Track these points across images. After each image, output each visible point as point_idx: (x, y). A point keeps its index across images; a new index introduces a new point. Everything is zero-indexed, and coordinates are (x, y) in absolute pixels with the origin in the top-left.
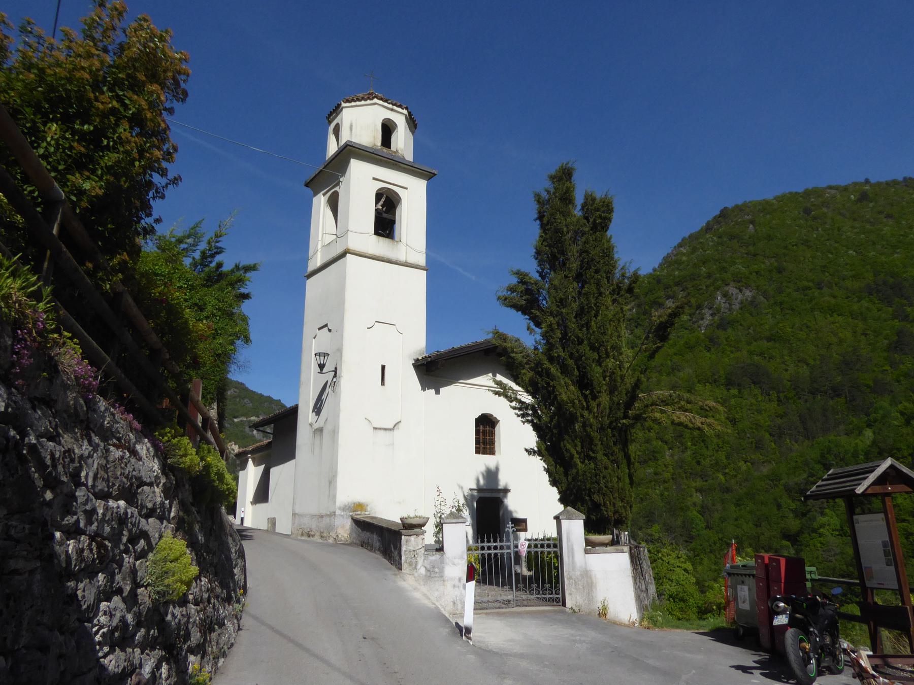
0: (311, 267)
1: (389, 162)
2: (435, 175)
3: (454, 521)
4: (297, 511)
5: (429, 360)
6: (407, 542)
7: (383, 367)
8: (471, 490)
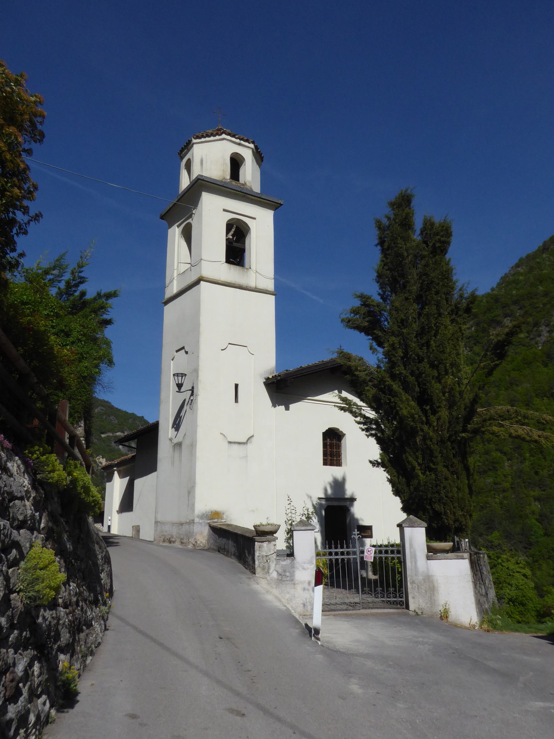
0: (168, 295)
1: (238, 194)
2: (281, 205)
3: (303, 528)
4: (159, 519)
5: (279, 378)
6: (260, 548)
7: (237, 386)
8: (319, 499)
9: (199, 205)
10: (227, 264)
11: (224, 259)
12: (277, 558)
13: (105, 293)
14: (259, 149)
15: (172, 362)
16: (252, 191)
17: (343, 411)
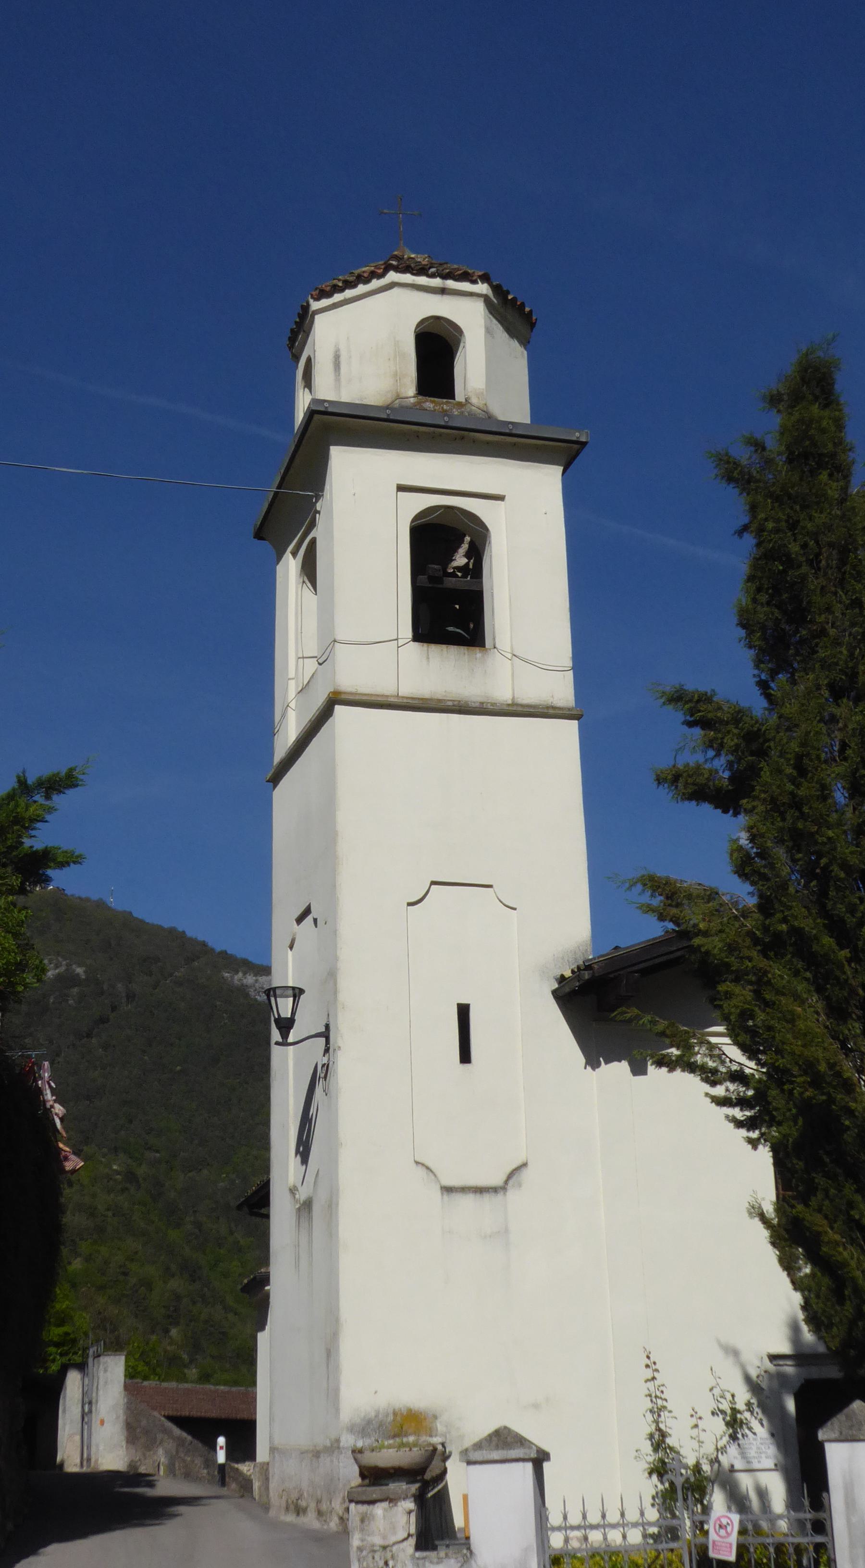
0: (280, 753)
1: (441, 435)
2: (584, 444)
3: (496, 1455)
4: (277, 1442)
5: (587, 975)
6: (362, 1521)
7: (463, 1012)
8: (773, 1358)
9: (327, 487)
10: (417, 644)
11: (406, 630)
12: (418, 1554)
13: (40, 778)
14: (508, 293)
15: (290, 953)
16: (490, 417)
17: (664, 1070)
